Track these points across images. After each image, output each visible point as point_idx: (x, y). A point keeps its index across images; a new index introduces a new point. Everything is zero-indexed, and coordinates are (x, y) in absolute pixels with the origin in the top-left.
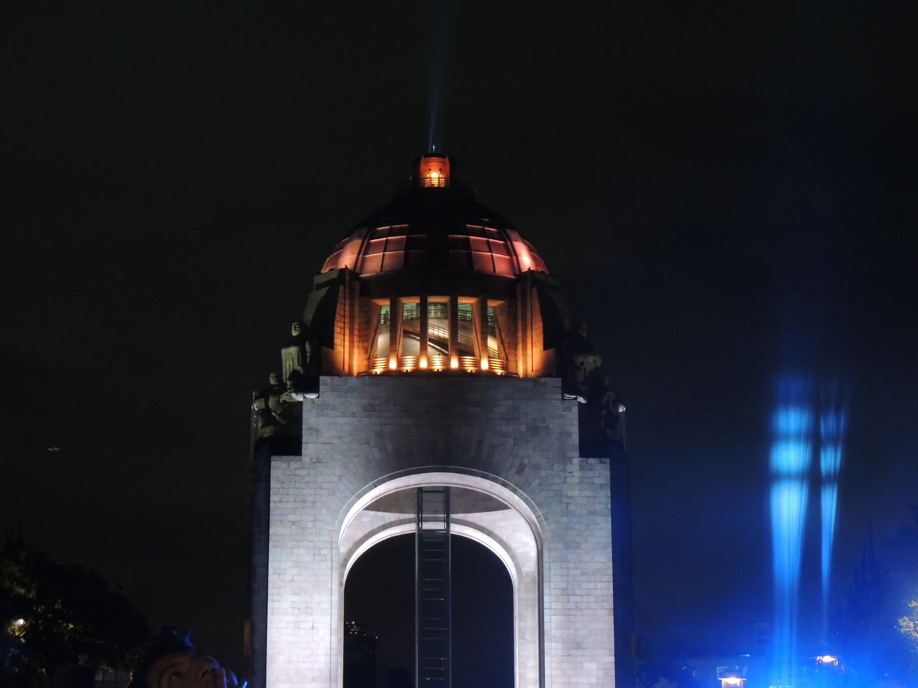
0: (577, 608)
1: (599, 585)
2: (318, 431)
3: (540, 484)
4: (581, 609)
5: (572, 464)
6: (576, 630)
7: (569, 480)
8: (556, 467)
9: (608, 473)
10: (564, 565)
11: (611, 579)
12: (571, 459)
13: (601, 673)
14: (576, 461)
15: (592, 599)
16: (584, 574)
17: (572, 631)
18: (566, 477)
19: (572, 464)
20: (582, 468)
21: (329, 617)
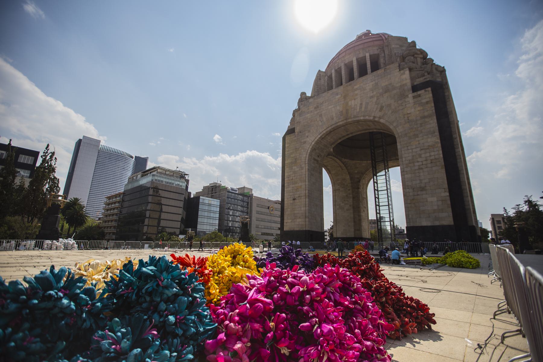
0: (419, 169)
1: (432, 154)
2: (300, 122)
3: (392, 112)
4: (422, 169)
5: (408, 97)
6: (420, 180)
7: (407, 106)
8: (400, 102)
9: (431, 95)
10: (409, 148)
11: (441, 149)
12: (407, 96)
13: (440, 203)
14: (411, 95)
15: (429, 162)
16: (422, 150)
17: (418, 182)
18: (406, 105)
19: (408, 97)
20: (414, 97)
21: (305, 191)
